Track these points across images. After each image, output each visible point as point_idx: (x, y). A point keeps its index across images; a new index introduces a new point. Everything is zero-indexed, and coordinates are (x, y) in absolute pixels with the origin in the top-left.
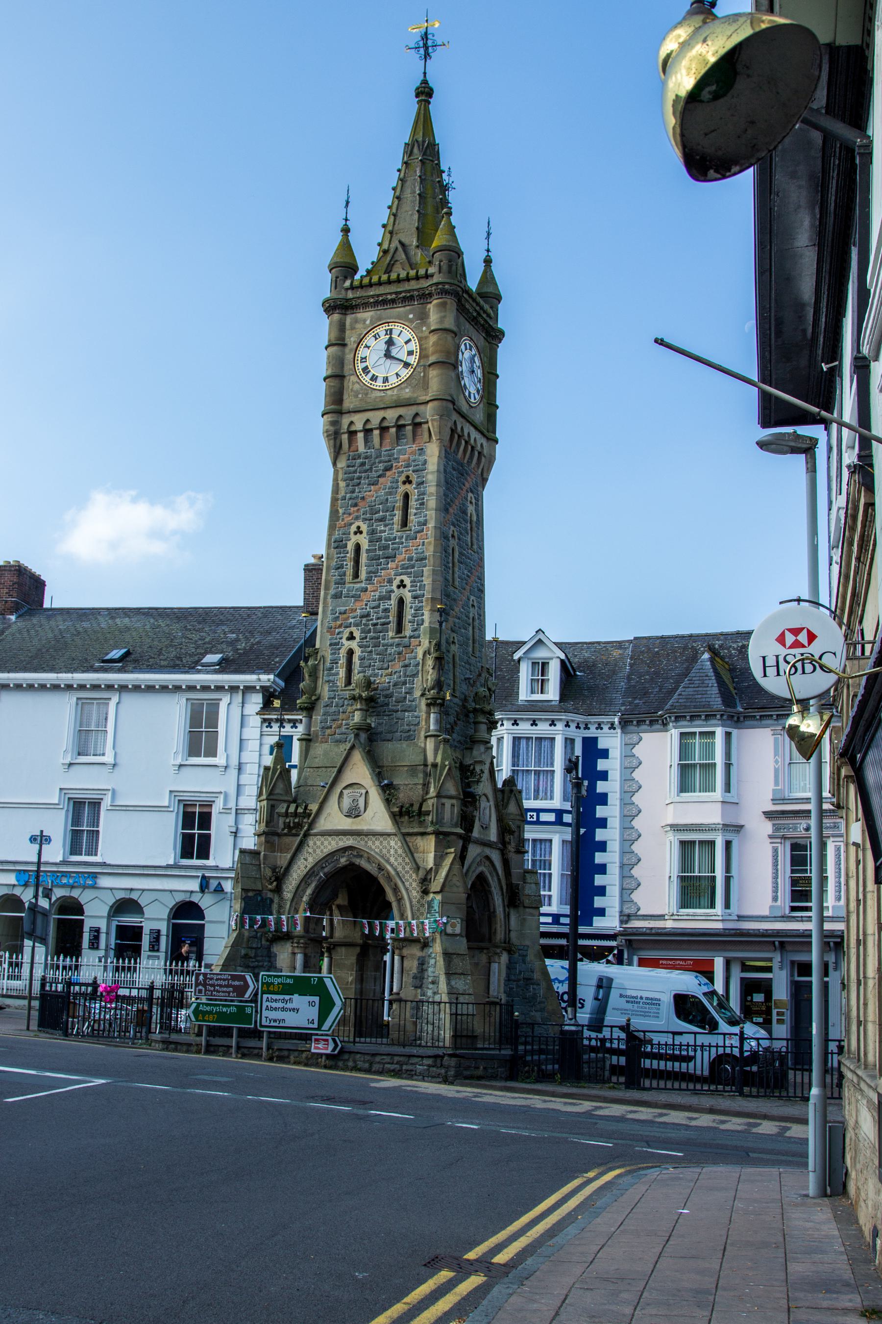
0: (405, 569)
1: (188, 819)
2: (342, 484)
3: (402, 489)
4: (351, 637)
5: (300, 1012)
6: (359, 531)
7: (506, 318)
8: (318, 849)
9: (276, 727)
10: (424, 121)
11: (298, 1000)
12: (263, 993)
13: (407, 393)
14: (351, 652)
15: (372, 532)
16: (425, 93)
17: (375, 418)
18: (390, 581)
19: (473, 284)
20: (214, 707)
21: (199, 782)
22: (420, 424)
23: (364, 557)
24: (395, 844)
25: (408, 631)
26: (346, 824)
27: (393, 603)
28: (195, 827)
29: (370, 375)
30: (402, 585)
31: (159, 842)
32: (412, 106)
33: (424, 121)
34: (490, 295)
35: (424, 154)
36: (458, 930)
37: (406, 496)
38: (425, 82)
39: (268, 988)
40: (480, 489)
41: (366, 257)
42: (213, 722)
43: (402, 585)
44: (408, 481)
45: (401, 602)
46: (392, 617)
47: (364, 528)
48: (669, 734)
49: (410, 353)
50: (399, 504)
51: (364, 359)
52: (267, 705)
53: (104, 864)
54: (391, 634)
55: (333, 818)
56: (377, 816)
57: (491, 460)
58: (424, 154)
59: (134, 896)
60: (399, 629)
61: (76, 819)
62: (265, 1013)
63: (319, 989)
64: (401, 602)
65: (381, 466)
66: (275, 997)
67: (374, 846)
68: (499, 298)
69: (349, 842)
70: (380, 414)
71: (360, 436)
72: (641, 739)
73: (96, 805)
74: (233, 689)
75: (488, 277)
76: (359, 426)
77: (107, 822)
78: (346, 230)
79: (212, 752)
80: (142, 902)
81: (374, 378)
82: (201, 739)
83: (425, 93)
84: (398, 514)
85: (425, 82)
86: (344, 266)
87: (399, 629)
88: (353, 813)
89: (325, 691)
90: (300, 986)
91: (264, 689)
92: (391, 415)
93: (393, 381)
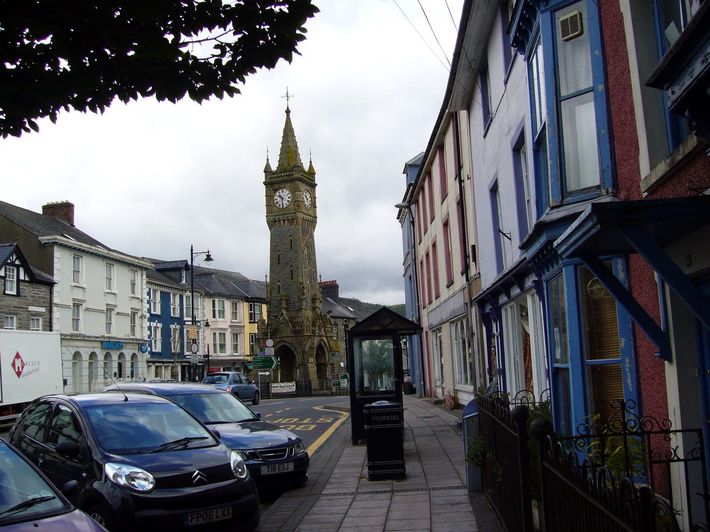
7: (318, 179)
16: (288, 112)
19: (306, 167)
34: (312, 173)
35: (288, 131)
36: (313, 361)
37: (291, 240)
38: (288, 108)
41: (274, 167)
49: (289, 198)
57: (316, 223)
58: (288, 131)
68: (315, 174)
75: (311, 167)
78: (268, 160)
83: (288, 112)
84: (289, 246)
85: (288, 108)
86: (267, 170)
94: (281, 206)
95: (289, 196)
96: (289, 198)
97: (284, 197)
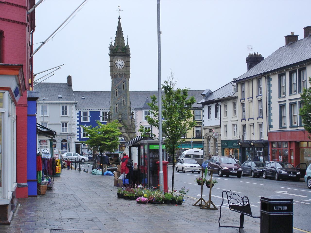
0: (124, 96)
2: (113, 83)
4: (117, 105)
9: (78, 110)
13: (123, 70)
15: (119, 90)
16: (119, 18)
17: (118, 73)
18: (122, 98)
20: (66, 107)
22: (125, 75)
23: (118, 94)
25: (125, 105)
27: (123, 100)
29: (117, 67)
38: (119, 17)
40: (127, 80)
42: (66, 109)
44: (123, 83)
45: (124, 100)
46: (123, 103)
47: (117, 89)
48: (142, 111)
49: (123, 64)
60: (124, 104)
64: (124, 100)
65: (119, 81)
71: (116, 76)
72: (137, 112)
76: (116, 74)
79: (66, 114)
80: (56, 140)
81: (118, 67)
82: (65, 112)
83: (119, 18)
85: (119, 17)
87: (124, 104)
94: (119, 68)
95: (123, 63)
96: (123, 64)
97: (120, 63)
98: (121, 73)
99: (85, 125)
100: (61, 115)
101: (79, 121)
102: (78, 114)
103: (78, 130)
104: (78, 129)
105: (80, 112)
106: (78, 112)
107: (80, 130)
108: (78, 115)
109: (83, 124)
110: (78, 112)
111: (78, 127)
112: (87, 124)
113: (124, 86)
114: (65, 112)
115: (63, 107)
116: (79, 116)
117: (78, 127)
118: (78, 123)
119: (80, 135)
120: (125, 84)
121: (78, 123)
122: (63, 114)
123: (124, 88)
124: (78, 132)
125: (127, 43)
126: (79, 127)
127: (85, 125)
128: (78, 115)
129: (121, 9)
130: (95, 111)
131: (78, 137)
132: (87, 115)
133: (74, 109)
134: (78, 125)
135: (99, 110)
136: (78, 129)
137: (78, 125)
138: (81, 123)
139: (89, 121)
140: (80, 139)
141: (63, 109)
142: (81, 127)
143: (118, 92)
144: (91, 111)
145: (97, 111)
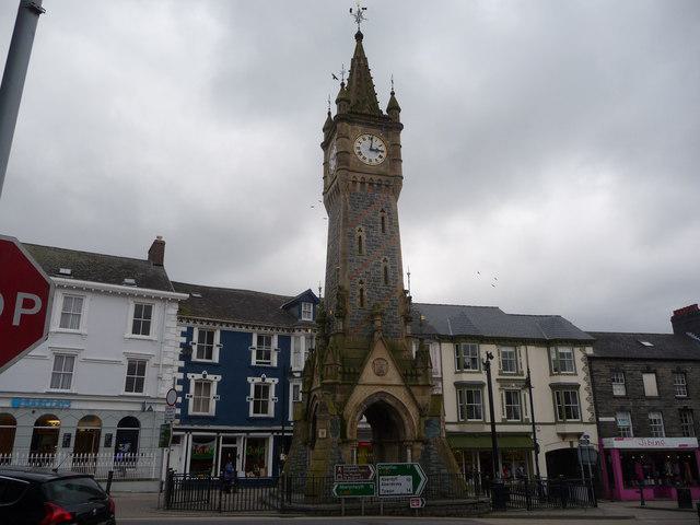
1: (131, 369)
3: (380, 214)
4: (361, 282)
5: (402, 485)
6: (360, 230)
8: (360, 395)
10: (359, 52)
11: (401, 479)
12: (380, 475)
13: (382, 169)
14: (362, 290)
16: (359, 37)
20: (149, 309)
21: (140, 347)
24: (402, 390)
26: (378, 380)
27: (382, 269)
28: (136, 373)
30: (385, 260)
31: (116, 382)
32: (354, 43)
33: (359, 52)
38: (359, 31)
39: (382, 473)
43: (385, 260)
44: (382, 211)
45: (386, 268)
47: (363, 229)
50: (380, 221)
51: (359, 148)
52: (180, 311)
53: (75, 394)
54: (382, 283)
55: (369, 375)
56: (393, 376)
58: (360, 65)
59: (95, 414)
61: (57, 366)
62: (381, 487)
63: (411, 471)
64: (386, 268)
66: (386, 477)
67: (391, 391)
69: (381, 389)
70: (369, 177)
73: (72, 358)
74: (165, 299)
77: (79, 369)
79: (146, 332)
82: (141, 326)
83: (359, 37)
85: (359, 31)
88: (380, 373)
89: (350, 309)
90: (403, 471)
91: (181, 303)
92: (375, 178)
93: (374, 162)
97: (367, 149)
98: (375, 178)
99: (205, 372)
100: (129, 334)
101: (185, 356)
102: (183, 334)
103: (179, 388)
104: (180, 382)
105: (190, 330)
106: (185, 329)
107: (186, 389)
108: (184, 340)
109: (197, 367)
110: (185, 329)
111: (181, 376)
112: (212, 369)
113: (363, 241)
114: (141, 326)
115: (138, 308)
116: (188, 341)
117: (181, 376)
118: (182, 364)
119: (184, 405)
120: (389, 214)
121: (182, 364)
122: (135, 331)
123: (387, 226)
124: (179, 394)
125: (393, 94)
126: (185, 375)
127: (205, 372)
128: (184, 340)
129: (364, 13)
130: (237, 329)
131: (178, 411)
132: (211, 340)
133: (175, 318)
134: (180, 370)
135: (250, 330)
136: (180, 382)
137: (180, 370)
138: (189, 366)
139: (216, 358)
140: (185, 418)
141: (137, 314)
142: (189, 376)
143: (364, 238)
144: (224, 327)
145: (244, 329)
